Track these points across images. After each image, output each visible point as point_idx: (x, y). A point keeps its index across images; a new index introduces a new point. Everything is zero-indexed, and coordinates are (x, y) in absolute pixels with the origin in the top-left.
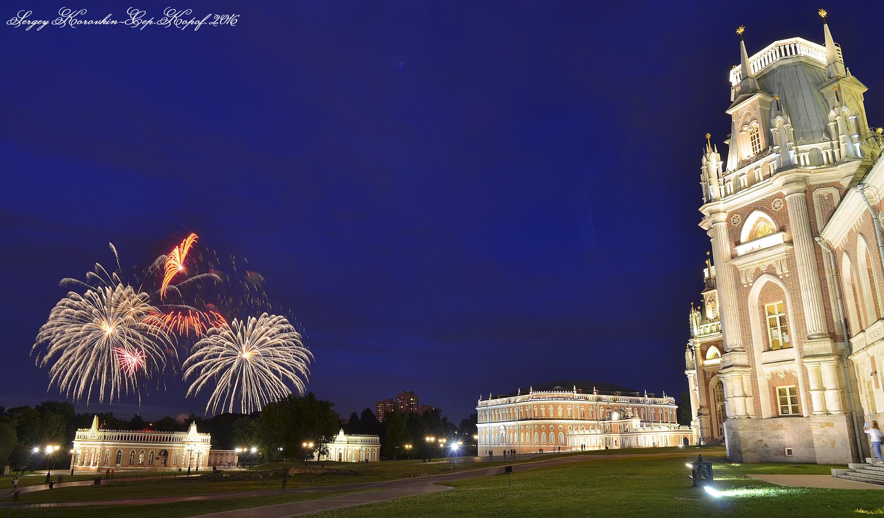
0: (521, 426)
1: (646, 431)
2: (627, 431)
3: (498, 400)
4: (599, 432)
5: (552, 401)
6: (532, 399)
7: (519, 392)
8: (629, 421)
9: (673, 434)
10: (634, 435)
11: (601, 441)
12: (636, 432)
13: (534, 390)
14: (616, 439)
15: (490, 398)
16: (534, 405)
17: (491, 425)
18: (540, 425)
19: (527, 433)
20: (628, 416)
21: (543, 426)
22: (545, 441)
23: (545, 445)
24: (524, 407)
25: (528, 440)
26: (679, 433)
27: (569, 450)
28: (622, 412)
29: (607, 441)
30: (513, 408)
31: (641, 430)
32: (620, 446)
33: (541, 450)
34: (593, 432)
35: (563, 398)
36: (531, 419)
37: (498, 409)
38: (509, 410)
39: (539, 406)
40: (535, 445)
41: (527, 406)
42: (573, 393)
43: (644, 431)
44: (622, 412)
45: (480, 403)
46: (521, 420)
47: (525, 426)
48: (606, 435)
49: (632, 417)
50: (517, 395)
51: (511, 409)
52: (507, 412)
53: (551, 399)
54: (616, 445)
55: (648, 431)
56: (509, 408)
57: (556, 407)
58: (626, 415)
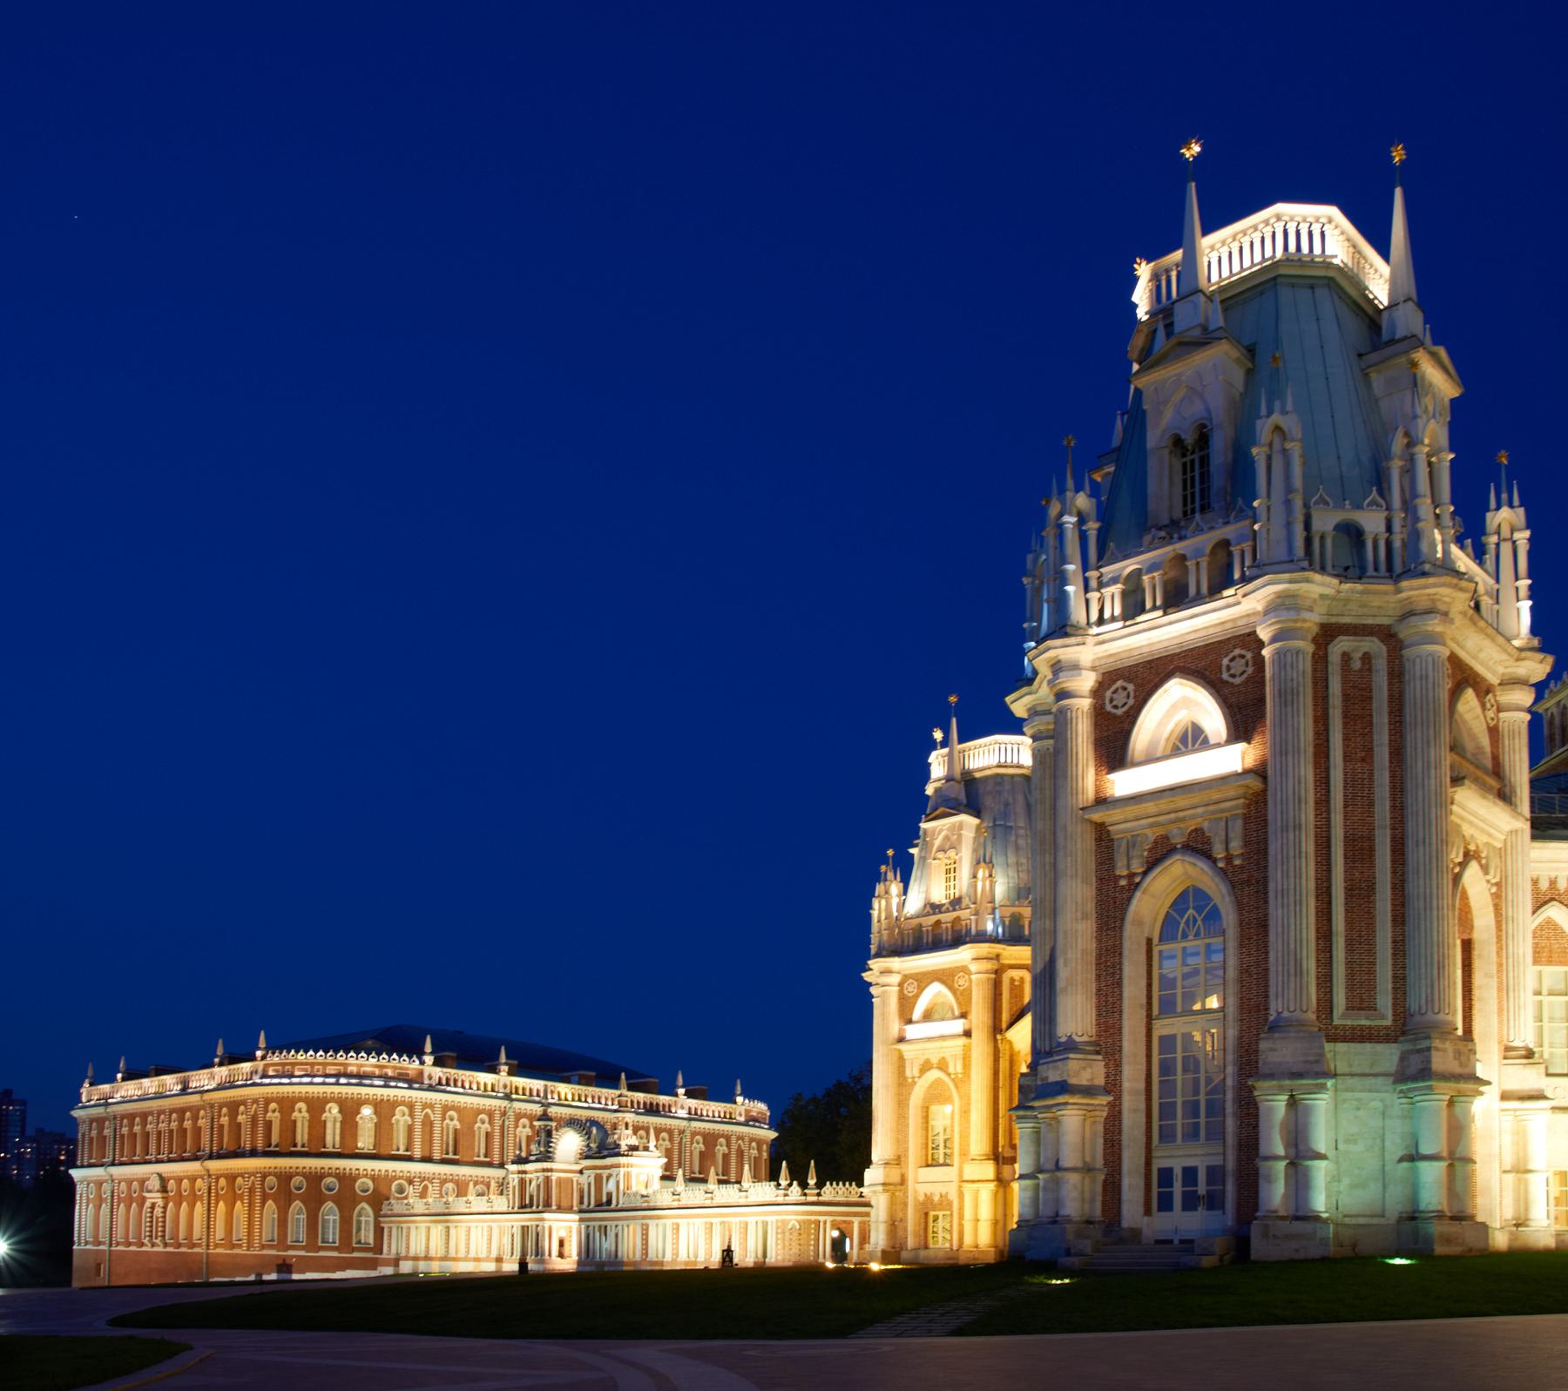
0: (217, 1179)
1: (684, 1202)
2: (609, 1202)
3: (146, 1082)
4: (501, 1203)
5: (336, 1089)
6: (264, 1076)
7: (220, 1051)
8: (618, 1166)
9: (793, 1216)
10: (634, 1218)
11: (507, 1241)
12: (645, 1207)
13: (273, 1047)
14: (563, 1234)
15: (119, 1076)
16: (268, 1101)
17: (117, 1171)
18: (285, 1177)
19: (239, 1203)
20: (618, 1146)
21: (297, 1180)
22: (302, 1236)
23: (303, 1248)
24: (234, 1107)
25: (240, 1230)
26: (821, 1213)
27: (388, 1271)
28: (594, 1130)
29: (532, 1241)
30: (195, 1111)
31: (665, 1198)
32: (575, 1257)
33: (284, 1267)
34: (479, 1204)
35: (379, 1077)
36: (253, 1153)
37: (144, 1116)
38: (181, 1120)
39: (287, 1104)
40: (263, 1247)
41: (243, 1103)
42: (422, 1063)
43: (676, 1204)
44: (594, 1130)
45: (85, 1090)
46: (220, 1156)
47: (231, 1178)
48: (526, 1219)
49: (634, 1148)
50: (211, 1065)
51: (188, 1114)
52: (174, 1125)
53: (332, 1080)
54: (561, 1255)
55: (690, 1203)
56: (181, 1112)
57: (350, 1109)
58: (610, 1140)
